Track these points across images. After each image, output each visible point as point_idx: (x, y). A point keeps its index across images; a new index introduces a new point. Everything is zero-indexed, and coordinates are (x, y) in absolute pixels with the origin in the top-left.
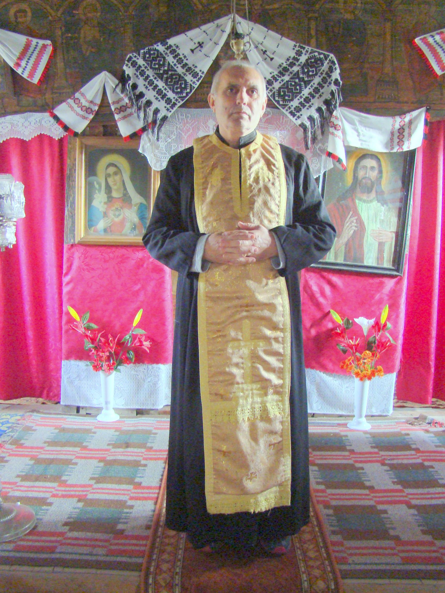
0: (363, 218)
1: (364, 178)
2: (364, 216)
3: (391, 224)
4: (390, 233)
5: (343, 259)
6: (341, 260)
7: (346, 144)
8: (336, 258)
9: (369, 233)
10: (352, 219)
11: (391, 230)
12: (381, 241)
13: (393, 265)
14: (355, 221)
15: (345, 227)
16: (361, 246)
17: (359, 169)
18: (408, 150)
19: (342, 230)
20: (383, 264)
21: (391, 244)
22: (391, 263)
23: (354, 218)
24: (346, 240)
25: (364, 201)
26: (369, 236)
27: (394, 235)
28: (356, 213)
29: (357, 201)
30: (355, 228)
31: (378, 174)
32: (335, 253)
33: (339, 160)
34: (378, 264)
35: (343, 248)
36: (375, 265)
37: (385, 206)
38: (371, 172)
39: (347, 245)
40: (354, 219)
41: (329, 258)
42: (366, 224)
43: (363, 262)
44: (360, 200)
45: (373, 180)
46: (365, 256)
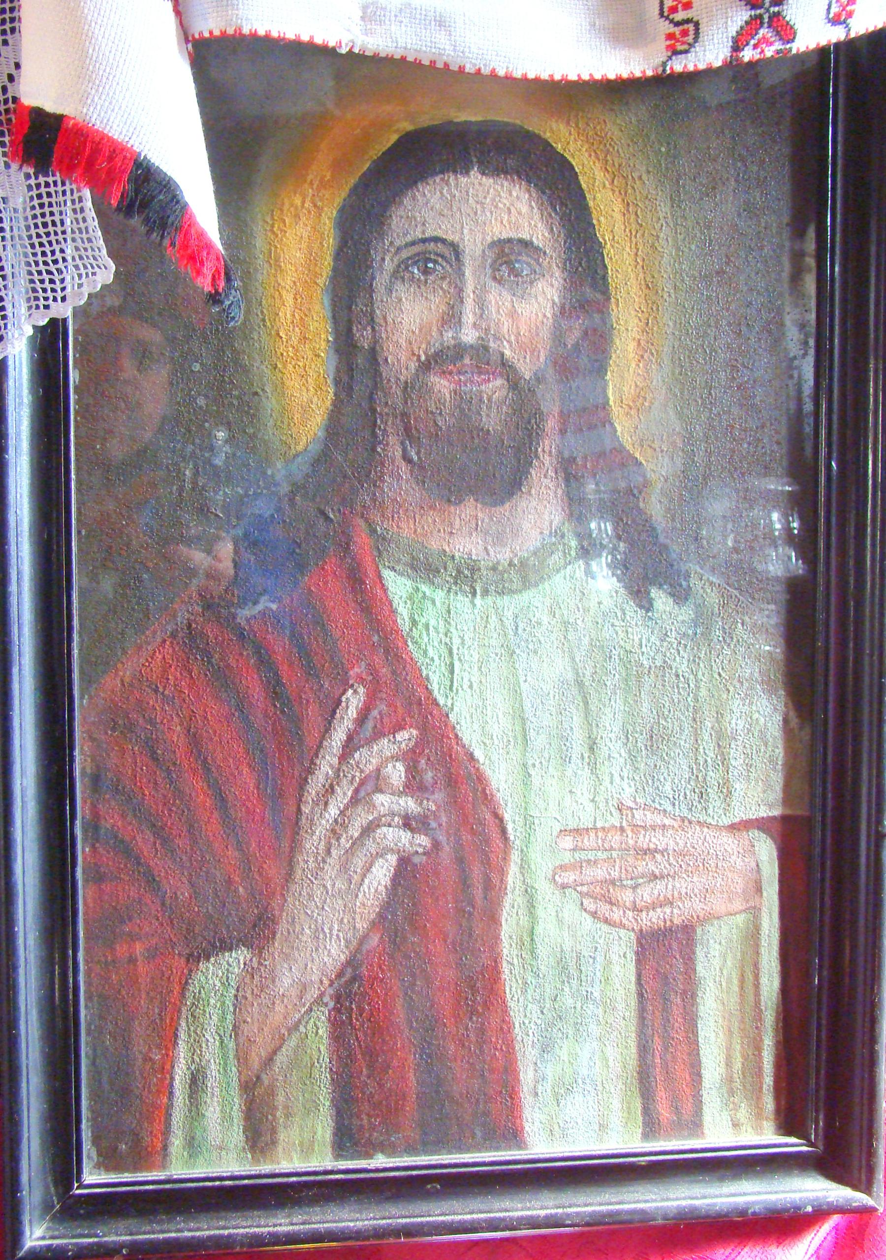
0: (469, 733)
1: (440, 360)
2: (478, 719)
3: (737, 762)
4: (729, 843)
5: (323, 1128)
6: (306, 1148)
7: (208, 24)
8: (259, 1134)
9: (542, 863)
10: (368, 758)
11: (739, 814)
12: (653, 919)
13: (789, 1121)
14: (397, 773)
15: (313, 841)
16: (480, 991)
17: (381, 281)
18: (837, 34)
19: (289, 876)
20: (695, 1126)
21: (753, 935)
22: (769, 1103)
23: (385, 746)
24: (334, 953)
25: (467, 577)
26: (544, 889)
27: (766, 852)
28: (408, 703)
29: (398, 586)
30: (405, 837)
31: (564, 312)
32: (249, 1087)
33: (138, 197)
34: (651, 1127)
35: (319, 1028)
36: (623, 1138)
37: (661, 600)
38: (499, 299)
39: (356, 1003)
40: (386, 756)
41: (192, 1145)
42: (500, 777)
43: (514, 1134)
44: (425, 568)
45: (526, 370)
46: (527, 1076)
